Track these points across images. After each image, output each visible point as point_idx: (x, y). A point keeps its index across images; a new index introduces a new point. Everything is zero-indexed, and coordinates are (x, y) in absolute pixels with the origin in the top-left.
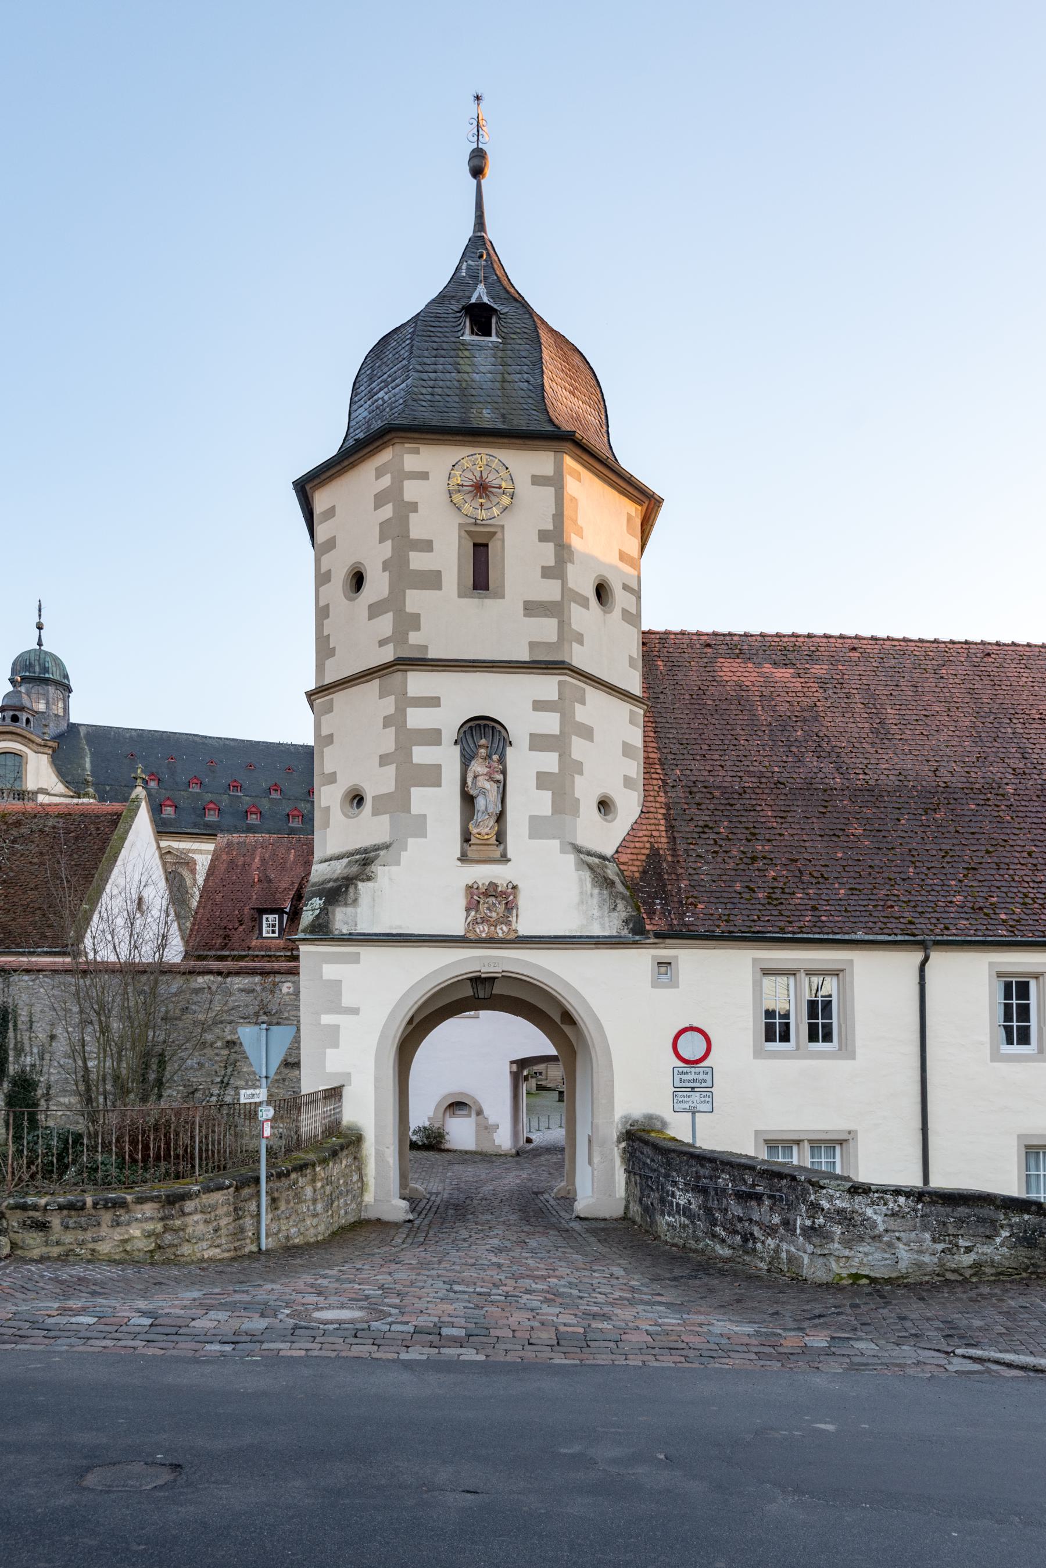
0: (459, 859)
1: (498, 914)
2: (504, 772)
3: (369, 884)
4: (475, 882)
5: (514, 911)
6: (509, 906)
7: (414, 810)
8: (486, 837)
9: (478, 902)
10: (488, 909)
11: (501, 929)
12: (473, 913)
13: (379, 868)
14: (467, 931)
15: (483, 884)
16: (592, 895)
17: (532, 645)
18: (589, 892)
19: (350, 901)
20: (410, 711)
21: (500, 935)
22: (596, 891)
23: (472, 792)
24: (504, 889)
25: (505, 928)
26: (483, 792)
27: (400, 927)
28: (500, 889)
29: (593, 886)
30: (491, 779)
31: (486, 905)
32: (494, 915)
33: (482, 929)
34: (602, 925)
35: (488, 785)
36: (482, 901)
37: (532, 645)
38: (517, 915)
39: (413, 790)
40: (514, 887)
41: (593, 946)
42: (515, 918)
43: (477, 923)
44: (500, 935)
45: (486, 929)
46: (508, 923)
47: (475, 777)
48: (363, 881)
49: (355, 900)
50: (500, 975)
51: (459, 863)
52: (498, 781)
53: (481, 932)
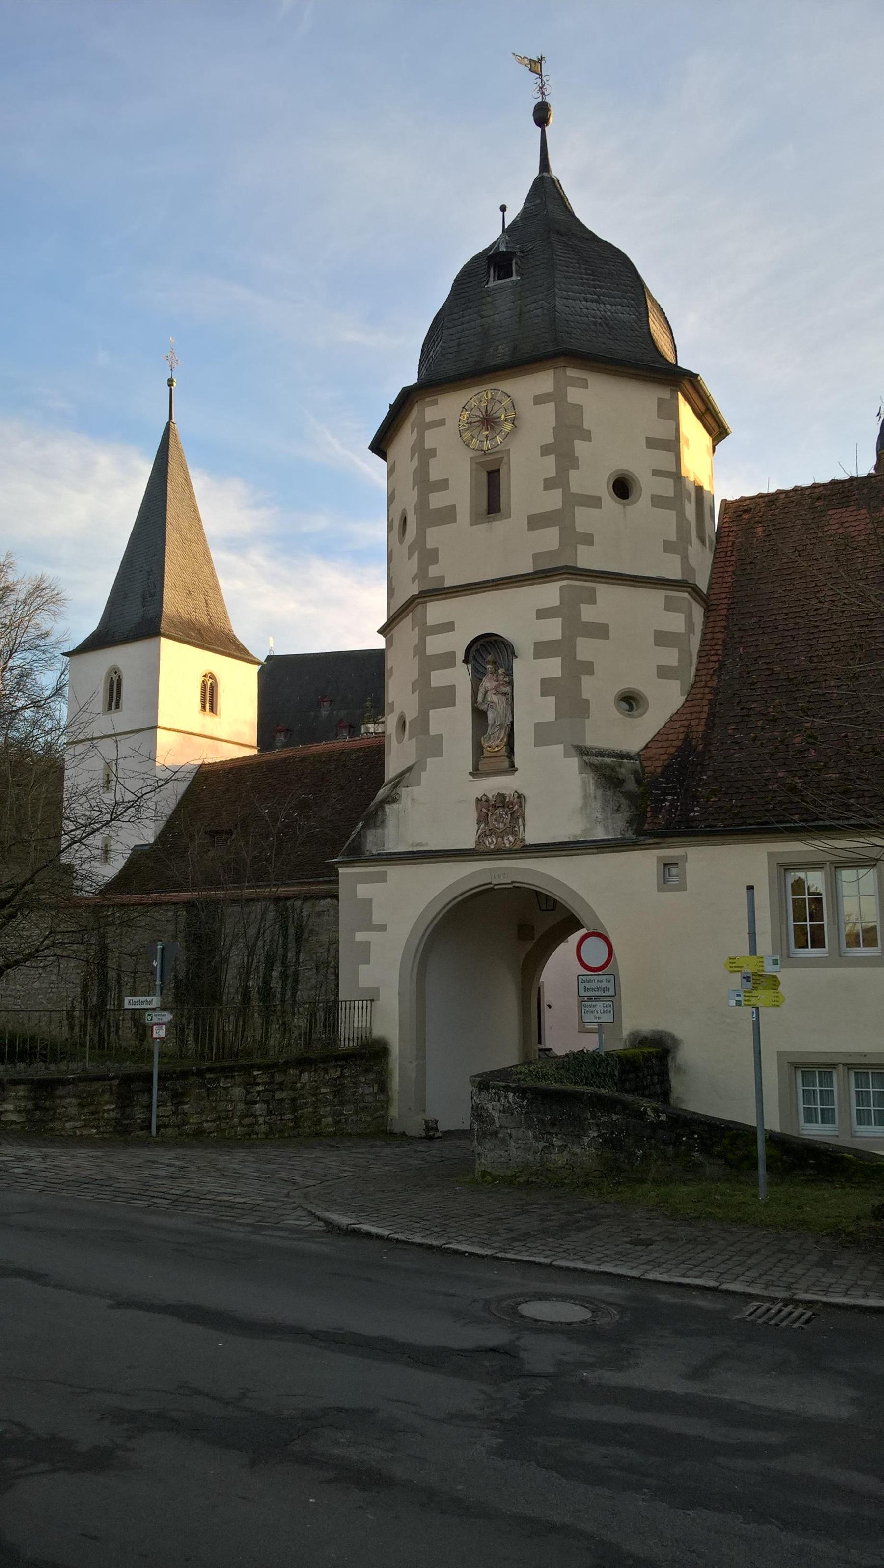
0: (470, 773)
1: (505, 825)
2: (511, 684)
3: (395, 806)
4: (485, 795)
5: (520, 821)
6: (515, 815)
7: (432, 733)
8: (496, 749)
9: (488, 815)
10: (496, 820)
11: (508, 839)
12: (483, 826)
13: (403, 789)
14: (478, 843)
15: (493, 796)
16: (595, 798)
17: (536, 557)
18: (592, 796)
19: (378, 823)
20: (429, 639)
21: (507, 845)
22: (600, 792)
23: (483, 707)
24: (512, 799)
25: (511, 838)
26: (492, 705)
27: (420, 844)
28: (507, 800)
29: (597, 787)
30: (497, 693)
31: (494, 817)
32: (501, 825)
33: (490, 841)
34: (606, 829)
35: (495, 699)
36: (490, 814)
37: (536, 557)
38: (524, 826)
39: (431, 712)
40: (519, 796)
41: (596, 851)
42: (521, 828)
43: (486, 835)
44: (507, 845)
45: (494, 840)
46: (514, 833)
47: (486, 692)
48: (389, 803)
49: (383, 822)
50: (511, 886)
51: (471, 778)
52: (505, 694)
53: (490, 844)
